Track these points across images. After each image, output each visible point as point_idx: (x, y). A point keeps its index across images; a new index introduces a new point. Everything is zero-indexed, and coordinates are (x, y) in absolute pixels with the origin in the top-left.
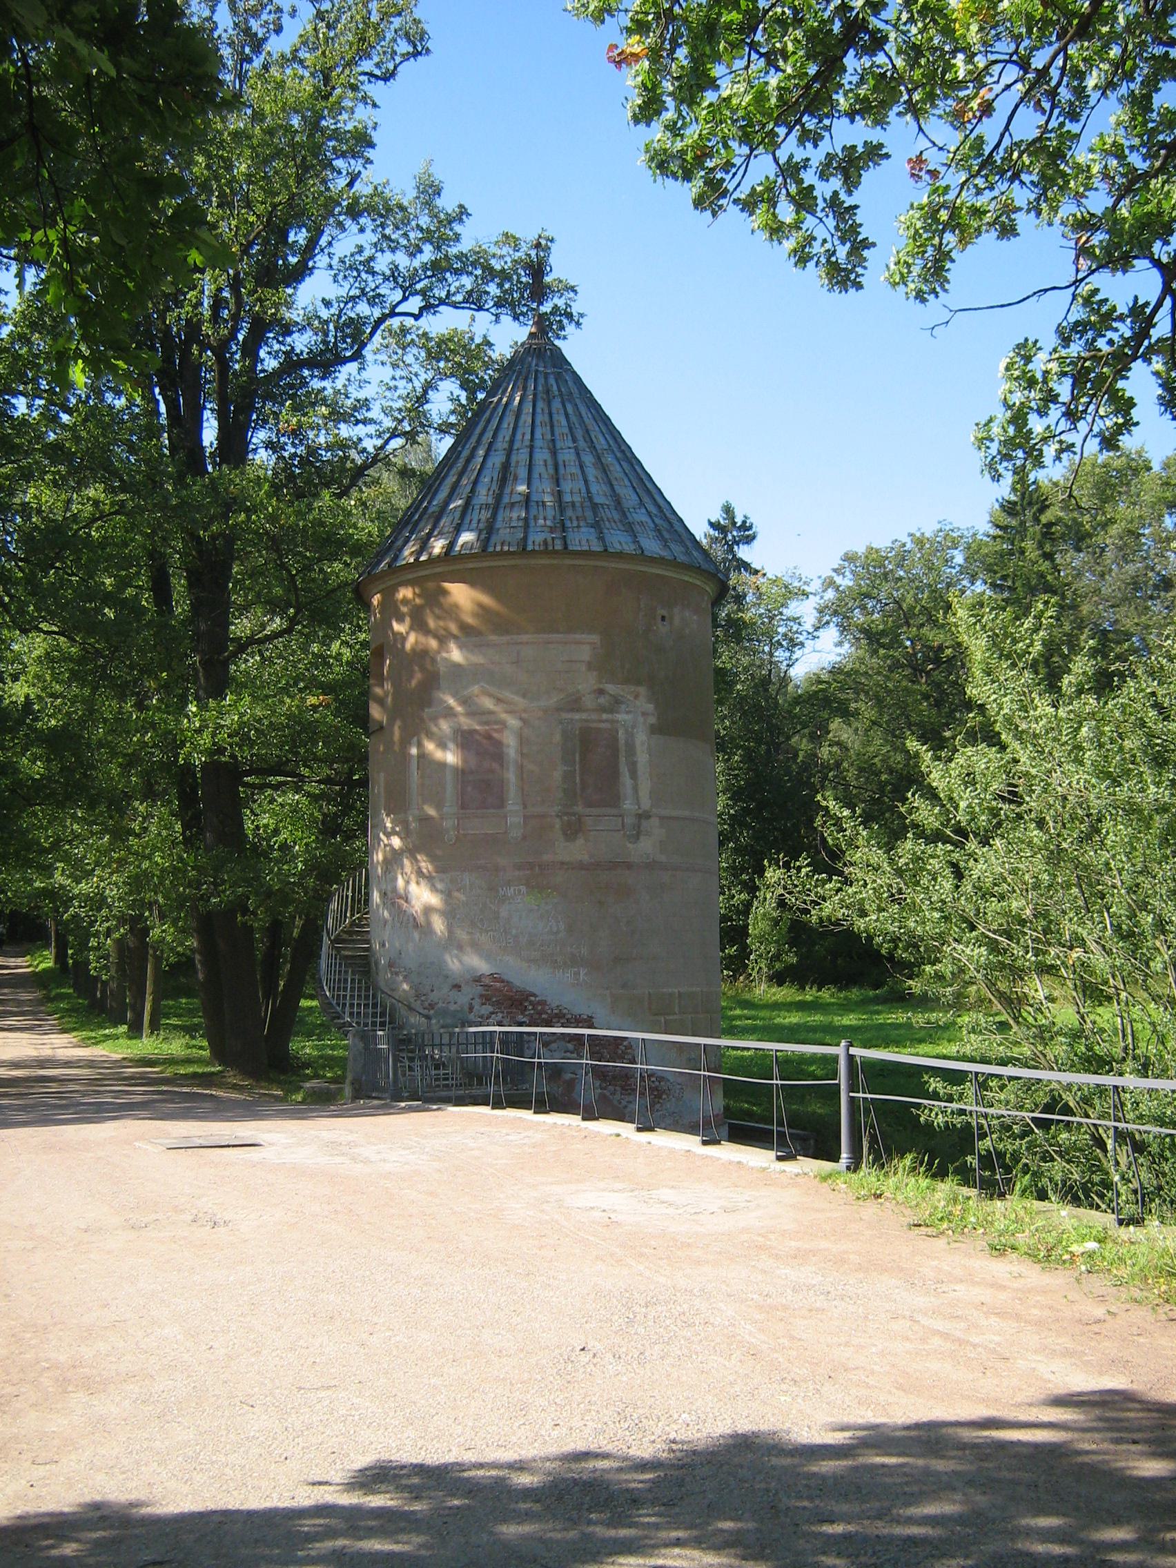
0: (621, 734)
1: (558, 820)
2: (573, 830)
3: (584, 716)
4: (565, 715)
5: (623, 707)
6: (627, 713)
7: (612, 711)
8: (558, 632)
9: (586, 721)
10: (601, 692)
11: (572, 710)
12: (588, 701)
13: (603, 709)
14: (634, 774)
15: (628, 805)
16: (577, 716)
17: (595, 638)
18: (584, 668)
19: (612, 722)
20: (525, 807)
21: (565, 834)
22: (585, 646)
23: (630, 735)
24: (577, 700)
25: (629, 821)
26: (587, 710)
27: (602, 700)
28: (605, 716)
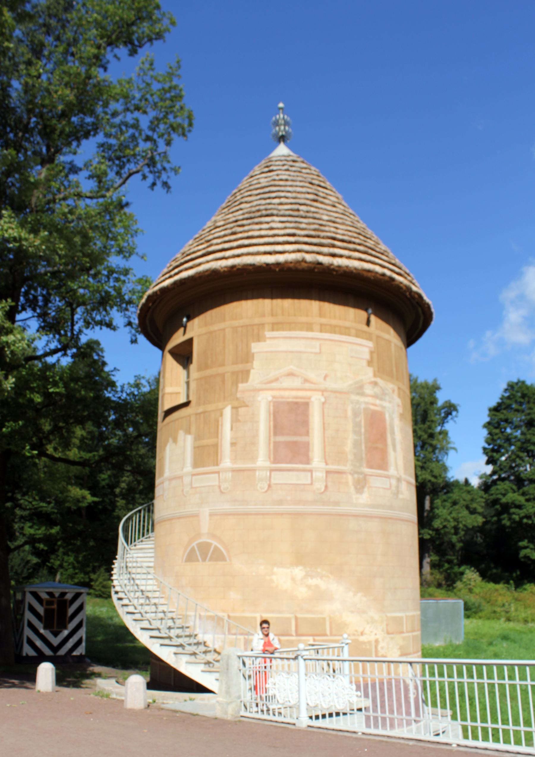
0: (387, 416)
1: (350, 477)
2: (361, 484)
3: (366, 399)
4: (354, 397)
5: (387, 398)
6: (390, 402)
7: (381, 399)
8: (349, 335)
9: (367, 403)
10: (375, 384)
11: (358, 394)
12: (369, 390)
13: (376, 396)
14: (394, 446)
15: (392, 471)
16: (362, 399)
17: (370, 344)
18: (364, 363)
19: (384, 407)
20: (327, 464)
21: (356, 488)
22: (364, 348)
23: (392, 419)
24: (361, 387)
25: (394, 482)
26: (367, 396)
27: (377, 390)
28: (378, 402)
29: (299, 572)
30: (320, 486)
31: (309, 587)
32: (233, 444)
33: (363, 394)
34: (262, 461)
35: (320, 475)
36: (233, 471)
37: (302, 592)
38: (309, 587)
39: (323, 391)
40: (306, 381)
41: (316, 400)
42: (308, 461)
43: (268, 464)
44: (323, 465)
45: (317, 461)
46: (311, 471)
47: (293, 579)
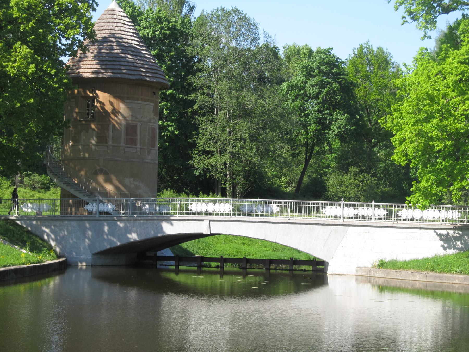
4: (149, 124)
18: (152, 111)
24: (151, 120)
29: (132, 179)
30: (139, 153)
31: (134, 184)
32: (113, 137)
33: (151, 123)
34: (122, 144)
35: (139, 149)
36: (113, 146)
37: (132, 186)
38: (134, 184)
39: (141, 122)
40: (136, 118)
41: (139, 124)
42: (136, 145)
43: (124, 145)
44: (140, 146)
45: (138, 145)
46: (136, 148)
47: (130, 182)
